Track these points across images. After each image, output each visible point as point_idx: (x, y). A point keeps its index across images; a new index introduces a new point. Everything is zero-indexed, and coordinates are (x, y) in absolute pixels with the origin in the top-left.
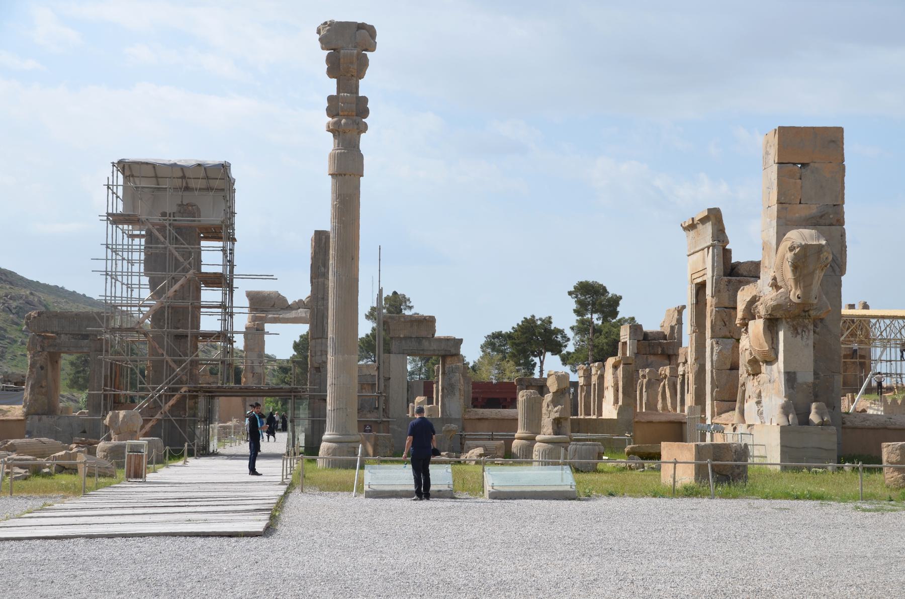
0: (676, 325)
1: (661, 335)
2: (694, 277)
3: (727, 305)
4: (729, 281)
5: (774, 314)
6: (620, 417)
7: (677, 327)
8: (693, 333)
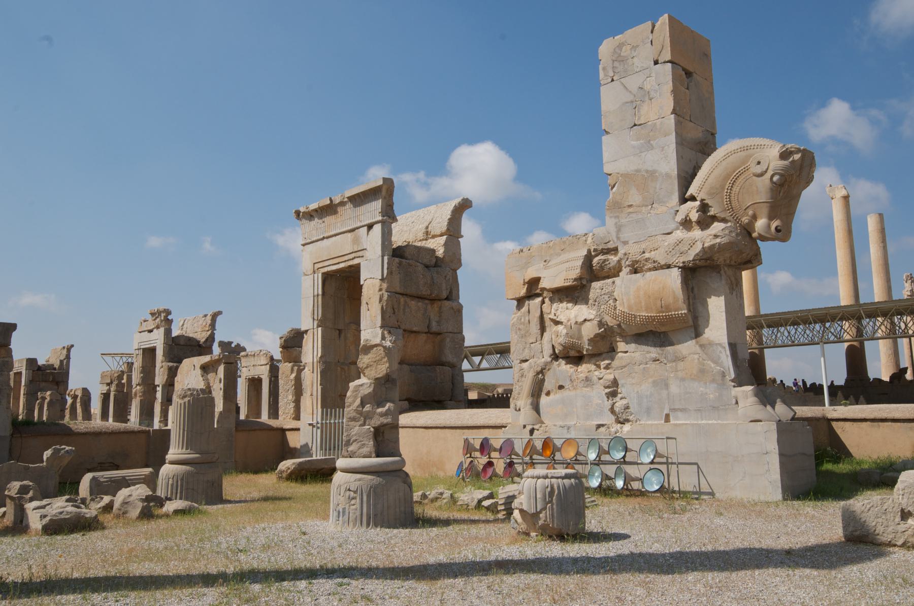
0: (65, 359)
1: (51, 367)
2: (317, 266)
3: (398, 290)
4: (400, 264)
5: (716, 259)
6: (220, 426)
7: (65, 361)
8: (318, 326)
